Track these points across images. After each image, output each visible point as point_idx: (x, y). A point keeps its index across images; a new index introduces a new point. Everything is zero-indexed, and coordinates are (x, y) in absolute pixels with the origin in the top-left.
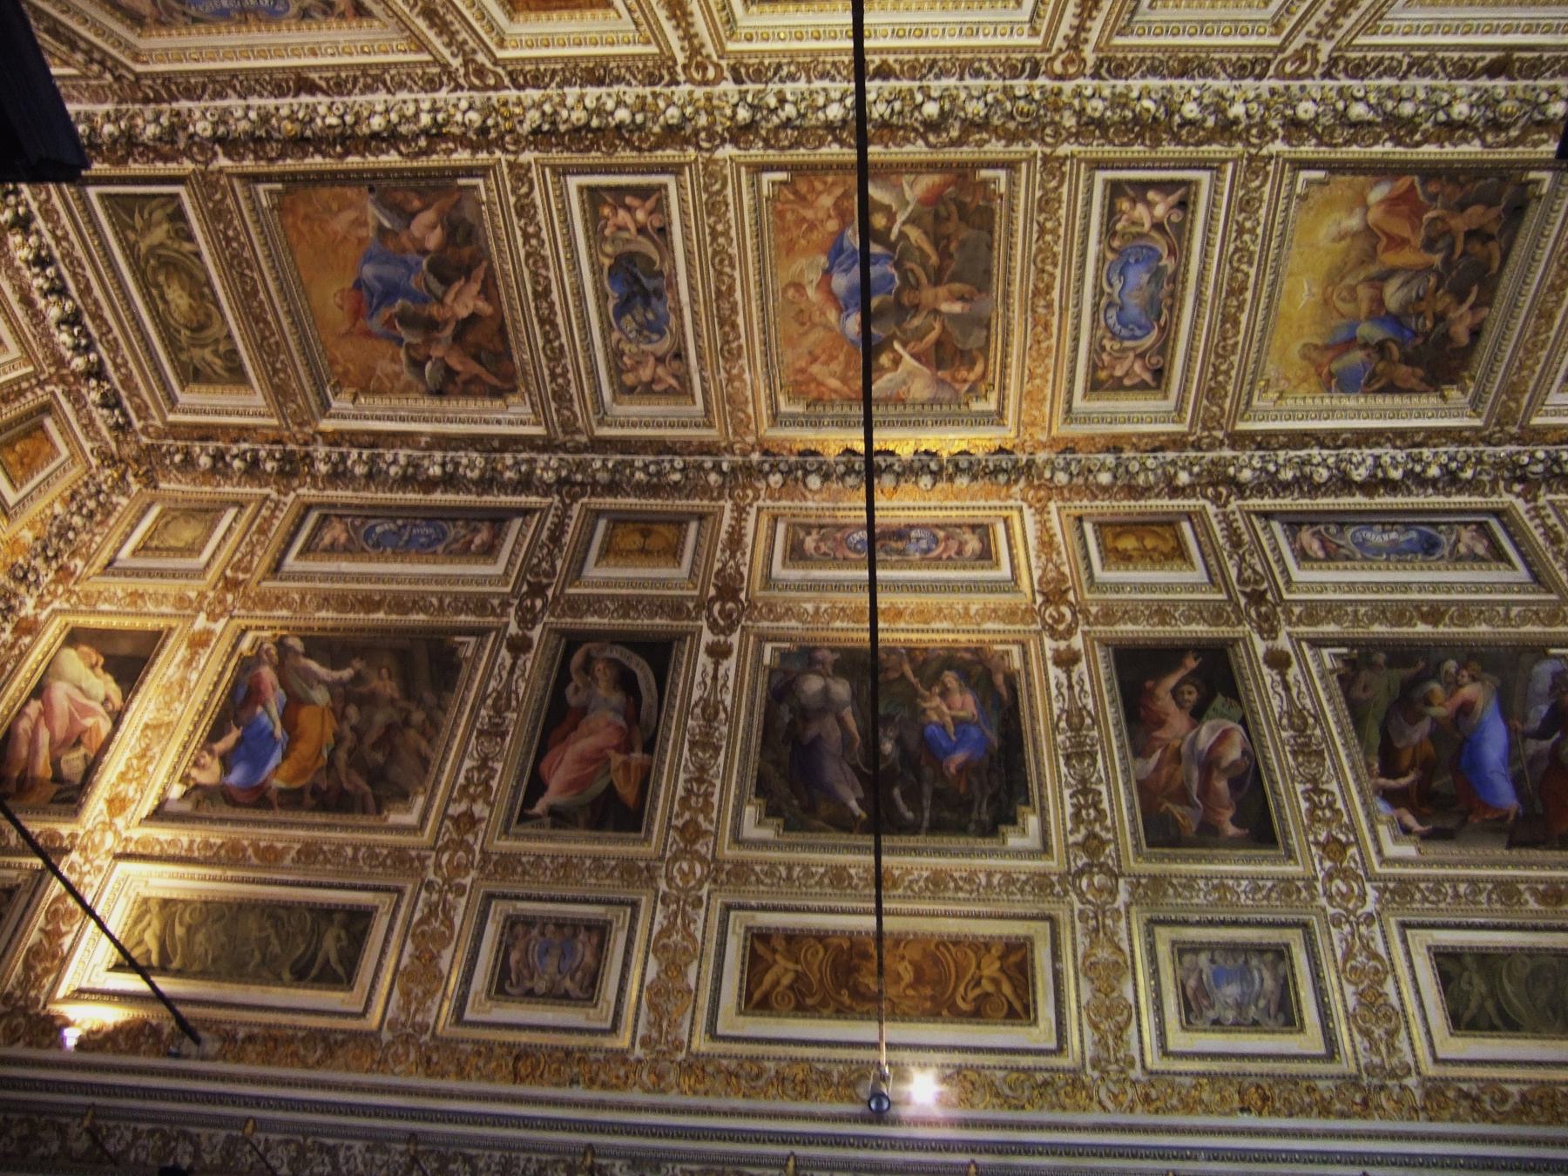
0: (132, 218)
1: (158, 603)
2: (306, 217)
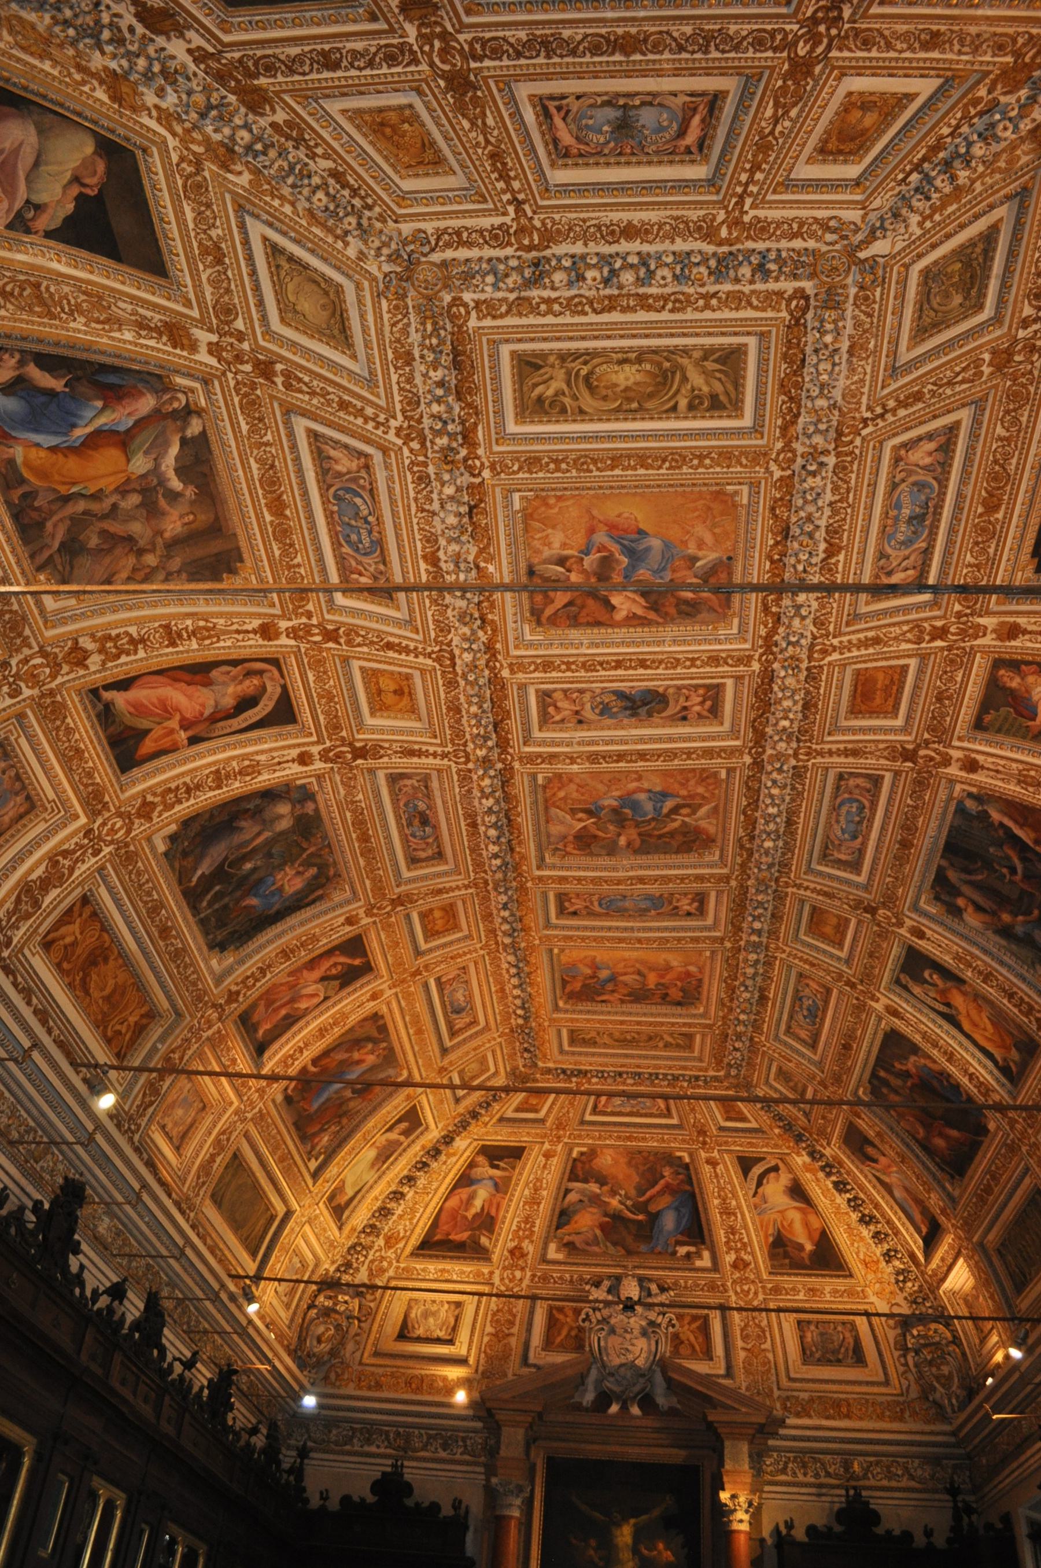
0: (716, 361)
1: (214, 283)
2: (709, 508)
